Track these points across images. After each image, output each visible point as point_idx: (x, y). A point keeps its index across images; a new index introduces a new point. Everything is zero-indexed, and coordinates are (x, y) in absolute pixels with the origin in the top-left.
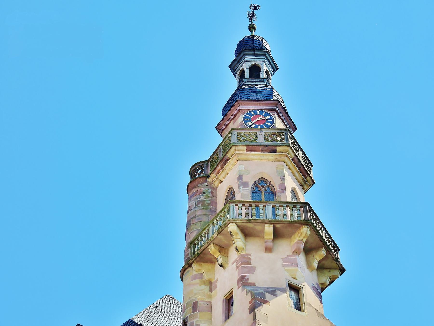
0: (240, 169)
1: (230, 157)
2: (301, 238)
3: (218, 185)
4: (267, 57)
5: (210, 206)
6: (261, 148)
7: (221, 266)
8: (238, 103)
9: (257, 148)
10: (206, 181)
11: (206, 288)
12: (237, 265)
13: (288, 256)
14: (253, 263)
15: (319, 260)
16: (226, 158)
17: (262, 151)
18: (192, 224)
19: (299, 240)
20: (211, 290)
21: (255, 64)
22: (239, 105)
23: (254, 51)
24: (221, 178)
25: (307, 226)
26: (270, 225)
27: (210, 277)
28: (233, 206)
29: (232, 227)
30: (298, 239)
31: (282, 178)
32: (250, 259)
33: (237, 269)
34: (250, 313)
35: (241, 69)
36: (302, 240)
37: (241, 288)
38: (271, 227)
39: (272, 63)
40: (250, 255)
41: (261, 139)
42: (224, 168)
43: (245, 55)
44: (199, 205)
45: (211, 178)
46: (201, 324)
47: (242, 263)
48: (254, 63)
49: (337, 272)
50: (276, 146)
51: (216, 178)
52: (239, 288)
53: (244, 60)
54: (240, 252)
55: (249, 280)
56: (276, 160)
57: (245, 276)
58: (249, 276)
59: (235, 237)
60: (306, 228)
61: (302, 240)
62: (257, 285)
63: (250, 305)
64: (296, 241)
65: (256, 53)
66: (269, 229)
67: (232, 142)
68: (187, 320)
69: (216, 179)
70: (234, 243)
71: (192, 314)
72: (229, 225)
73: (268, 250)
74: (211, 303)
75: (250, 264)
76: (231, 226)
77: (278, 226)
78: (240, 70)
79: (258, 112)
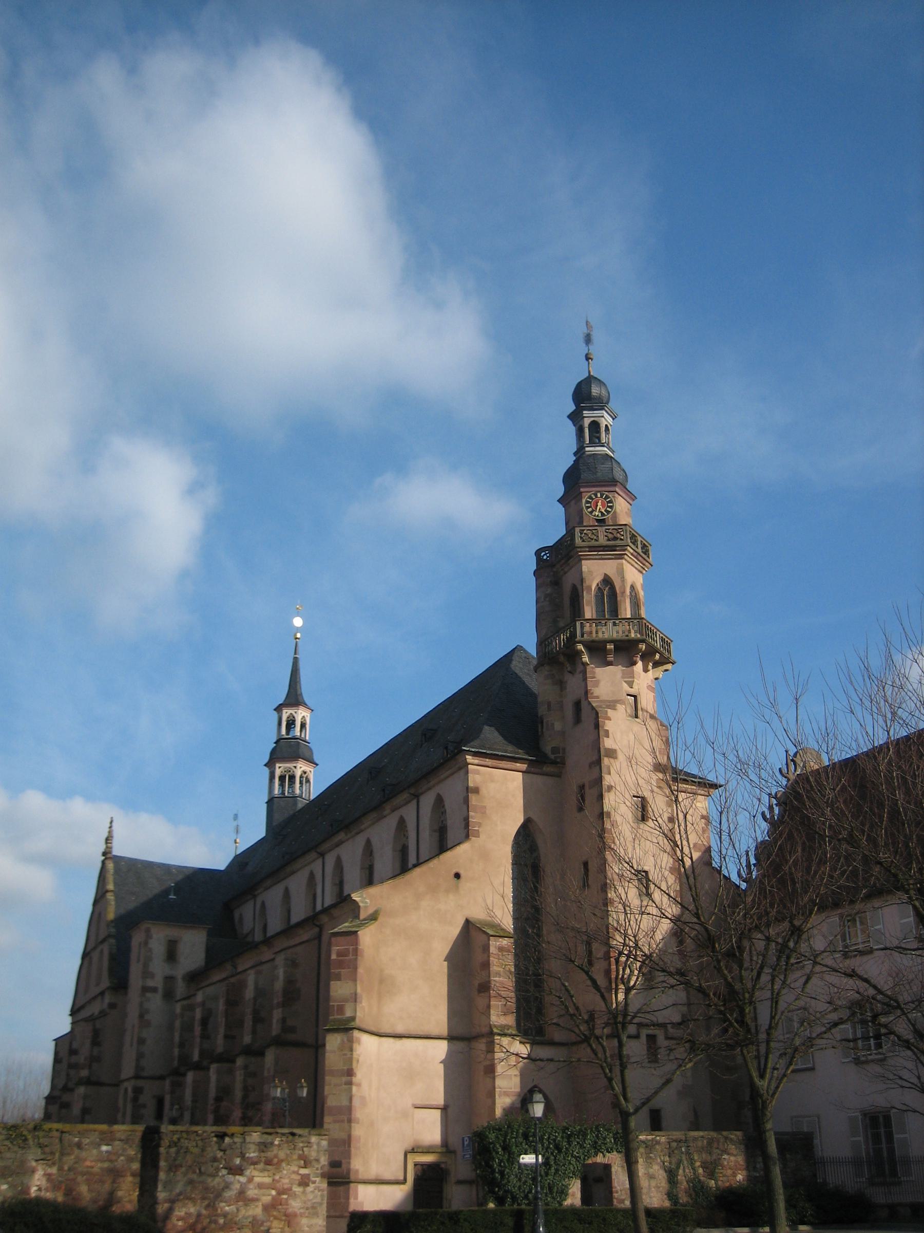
7: (570, 672)
20: (562, 691)
21: (594, 421)
24: (566, 570)
34: (595, 728)
44: (547, 599)
48: (592, 419)
62: (601, 698)
74: (562, 702)
77: (617, 643)
79: (599, 495)
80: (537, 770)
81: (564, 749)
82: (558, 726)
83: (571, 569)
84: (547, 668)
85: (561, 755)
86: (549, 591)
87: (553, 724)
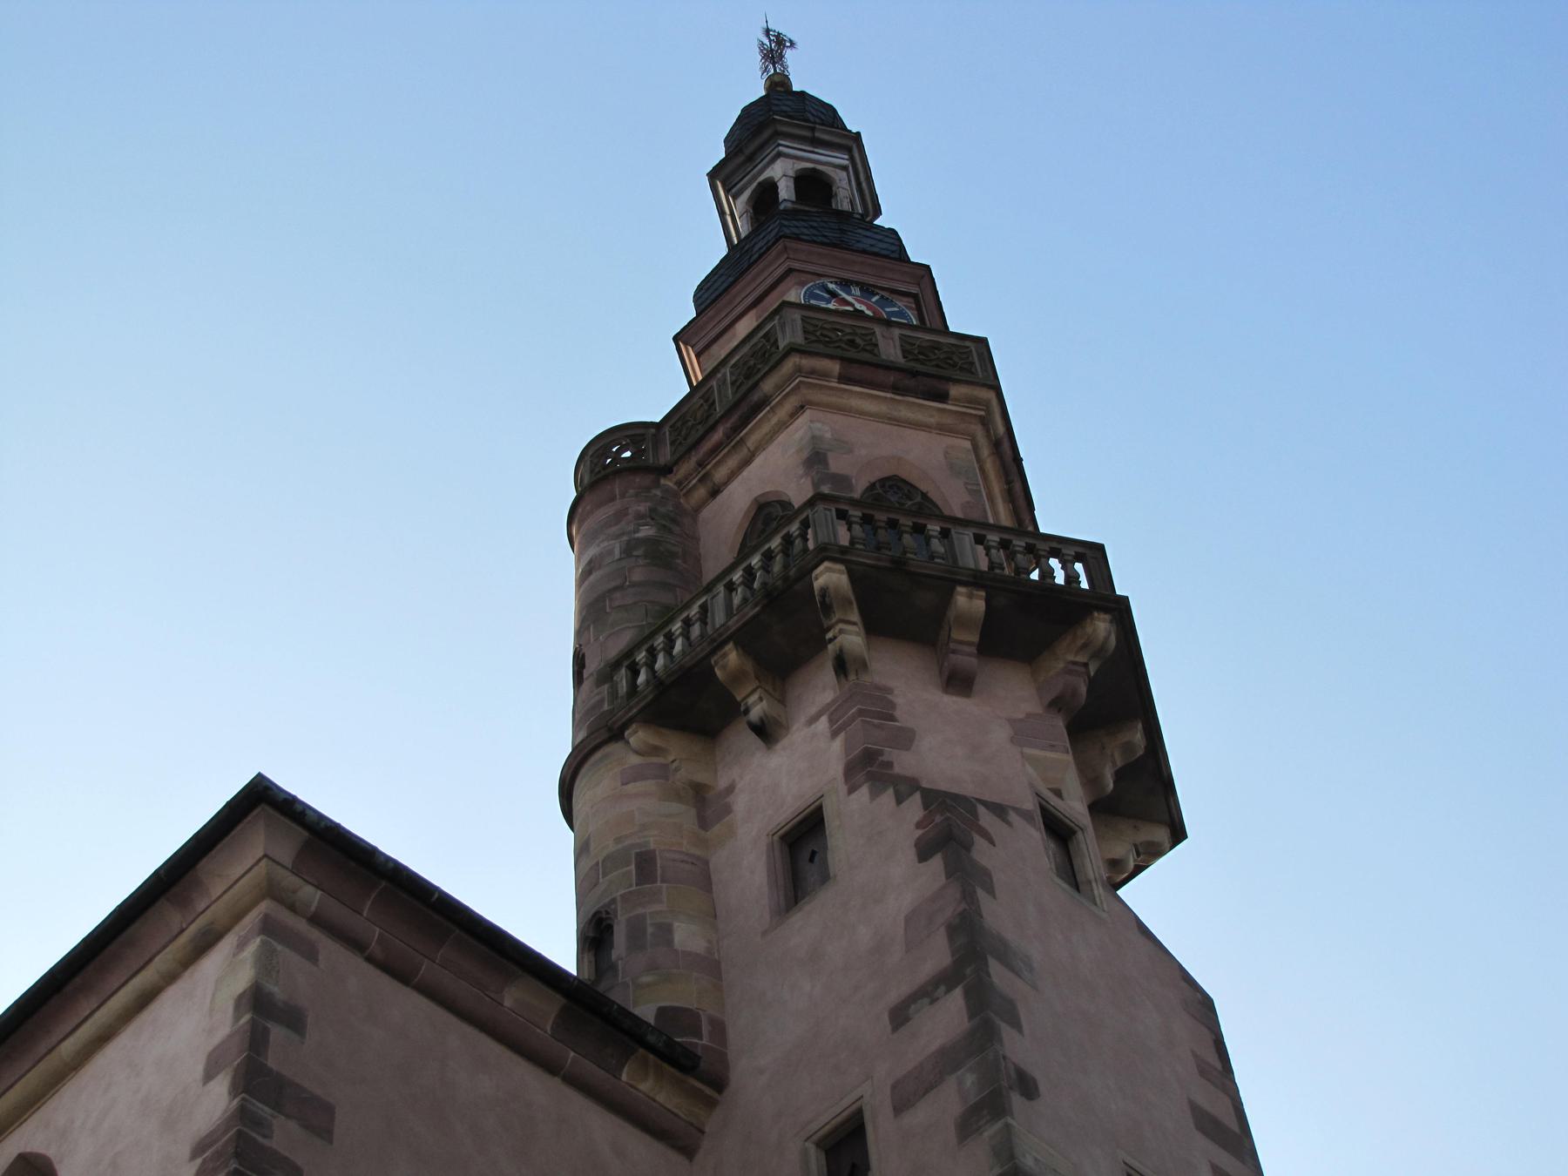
0: (817, 433)
1: (771, 396)
2: (1081, 659)
3: (703, 504)
4: (852, 159)
5: (679, 561)
6: (891, 378)
8: (785, 248)
9: (881, 376)
10: (657, 484)
11: (684, 814)
12: (831, 721)
13: (1029, 715)
14: (904, 717)
15: (1119, 764)
16: (756, 397)
17: (896, 389)
18: (611, 608)
19: (1074, 663)
20: (704, 823)
21: (814, 170)
22: (786, 256)
23: (813, 129)
24: (720, 474)
25: (1108, 617)
26: (975, 592)
27: (701, 777)
28: (828, 513)
29: (830, 577)
30: (1070, 657)
31: (969, 487)
32: (893, 705)
33: (834, 734)
35: (762, 178)
36: (1086, 665)
37: (864, 791)
38: (979, 597)
39: (864, 185)
40: (890, 690)
41: (890, 348)
42: (738, 438)
43: (778, 134)
45: (682, 470)
46: (676, 924)
47: (861, 713)
49: (1162, 834)
50: (949, 380)
51: (700, 476)
52: (851, 791)
53: (774, 152)
54: (852, 677)
55: (895, 765)
56: (942, 429)
57: (880, 753)
58: (890, 754)
59: (837, 616)
60: (1104, 621)
61: (1086, 665)
63: (920, 832)
64: (1061, 665)
65: (817, 134)
66: (969, 603)
67: (782, 344)
68: (615, 911)
69: (696, 479)
70: (831, 640)
71: (634, 888)
72: (821, 568)
73: (959, 683)
74: (707, 863)
75: (892, 718)
76: (828, 570)
78: (755, 184)
80: (591, 1070)
81: (719, 1028)
82: (687, 936)
83: (747, 462)
84: (638, 736)
85: (704, 1042)
86: (646, 531)
87: (665, 931)
